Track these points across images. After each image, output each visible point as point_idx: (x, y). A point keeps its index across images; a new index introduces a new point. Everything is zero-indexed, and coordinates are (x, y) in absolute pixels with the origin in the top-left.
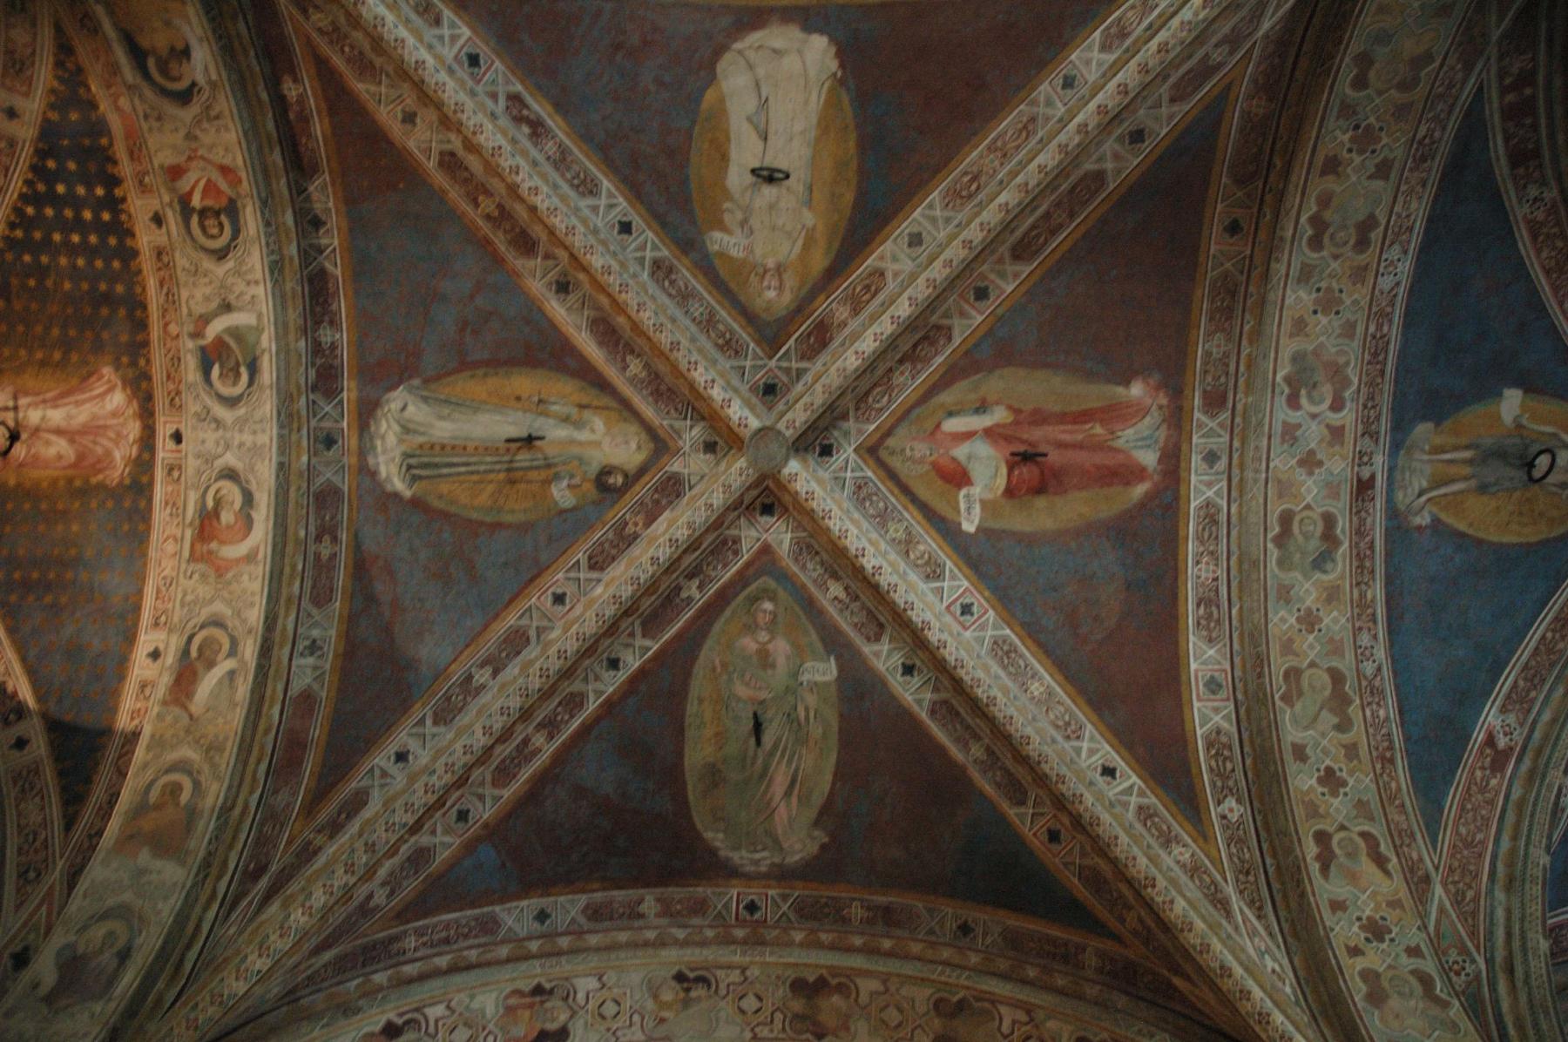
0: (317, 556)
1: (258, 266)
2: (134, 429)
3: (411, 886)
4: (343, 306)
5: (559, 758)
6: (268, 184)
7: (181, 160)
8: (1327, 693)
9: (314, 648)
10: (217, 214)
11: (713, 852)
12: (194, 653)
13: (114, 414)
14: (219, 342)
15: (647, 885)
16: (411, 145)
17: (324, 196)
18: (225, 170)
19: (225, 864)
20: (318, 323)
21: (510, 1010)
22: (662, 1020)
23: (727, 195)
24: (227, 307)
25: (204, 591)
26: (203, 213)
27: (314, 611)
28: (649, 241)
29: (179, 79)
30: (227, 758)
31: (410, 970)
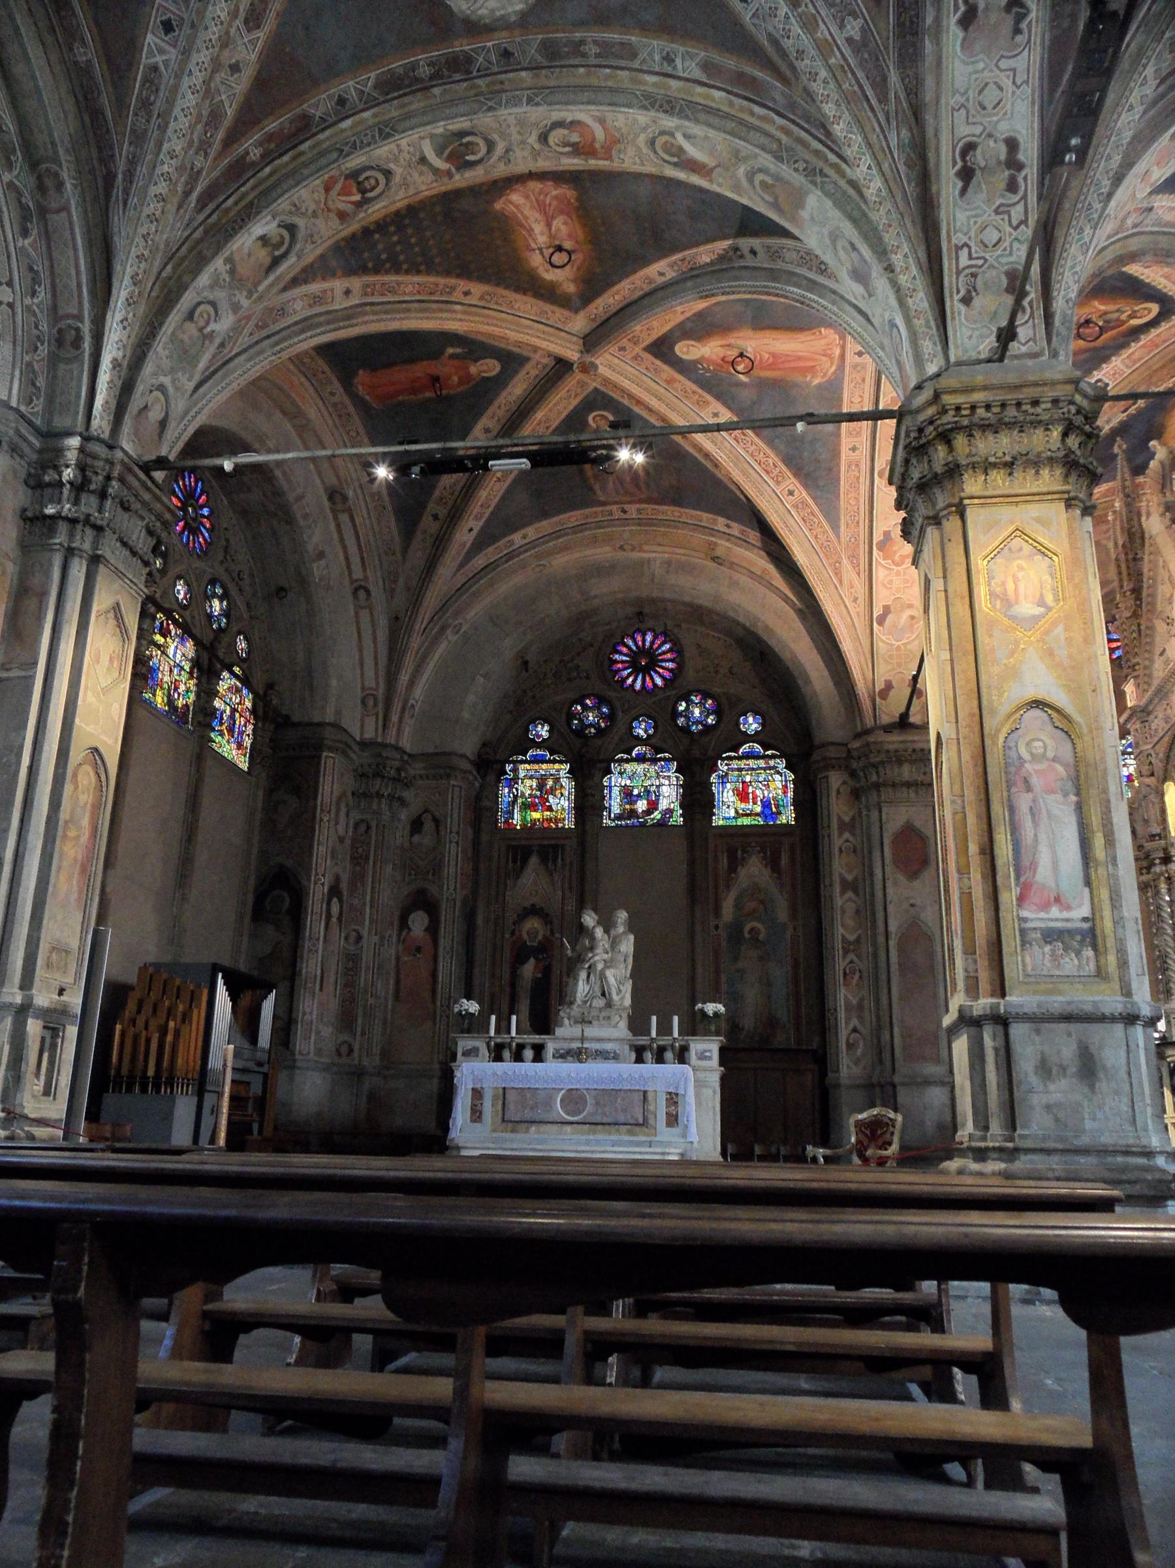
0: (597, 56)
1: (386, 148)
2: (534, 186)
4: (397, 65)
6: (328, 151)
7: (333, 215)
9: (669, 59)
10: (359, 183)
12: (675, 160)
13: (527, 197)
14: (449, 159)
16: (253, 57)
17: (319, 104)
18: (327, 190)
19: (817, 153)
20: (417, 80)
24: (423, 160)
25: (631, 151)
26: (363, 192)
27: (640, 57)
29: (282, 237)
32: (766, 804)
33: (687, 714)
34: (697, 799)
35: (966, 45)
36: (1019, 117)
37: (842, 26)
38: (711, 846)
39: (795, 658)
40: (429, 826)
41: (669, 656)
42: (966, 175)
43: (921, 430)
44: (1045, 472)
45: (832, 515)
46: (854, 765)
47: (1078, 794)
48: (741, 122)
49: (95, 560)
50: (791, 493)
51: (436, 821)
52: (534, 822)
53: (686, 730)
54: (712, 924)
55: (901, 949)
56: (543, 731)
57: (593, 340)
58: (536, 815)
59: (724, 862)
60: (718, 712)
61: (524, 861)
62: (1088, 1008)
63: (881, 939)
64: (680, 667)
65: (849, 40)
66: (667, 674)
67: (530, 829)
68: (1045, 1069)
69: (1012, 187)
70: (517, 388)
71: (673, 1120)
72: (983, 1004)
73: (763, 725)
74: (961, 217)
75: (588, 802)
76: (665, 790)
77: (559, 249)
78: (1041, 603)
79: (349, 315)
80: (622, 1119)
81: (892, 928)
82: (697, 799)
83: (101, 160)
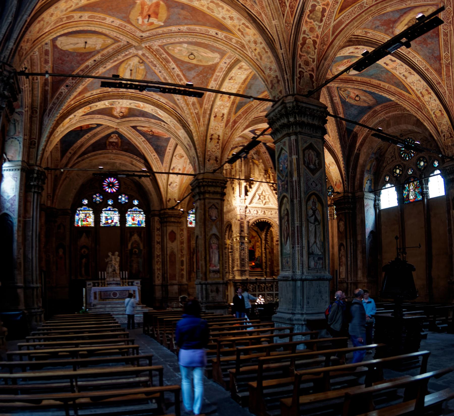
8: (215, 5)
11: (213, 64)
21: (222, 100)
30: (171, 118)
32: (139, 222)
34: (123, 220)
35: (214, 120)
39: (149, 190)
45: (162, 162)
46: (161, 216)
53: (121, 203)
55: (170, 258)
59: (129, 235)
60: (128, 199)
63: (165, 255)
82: (123, 220)
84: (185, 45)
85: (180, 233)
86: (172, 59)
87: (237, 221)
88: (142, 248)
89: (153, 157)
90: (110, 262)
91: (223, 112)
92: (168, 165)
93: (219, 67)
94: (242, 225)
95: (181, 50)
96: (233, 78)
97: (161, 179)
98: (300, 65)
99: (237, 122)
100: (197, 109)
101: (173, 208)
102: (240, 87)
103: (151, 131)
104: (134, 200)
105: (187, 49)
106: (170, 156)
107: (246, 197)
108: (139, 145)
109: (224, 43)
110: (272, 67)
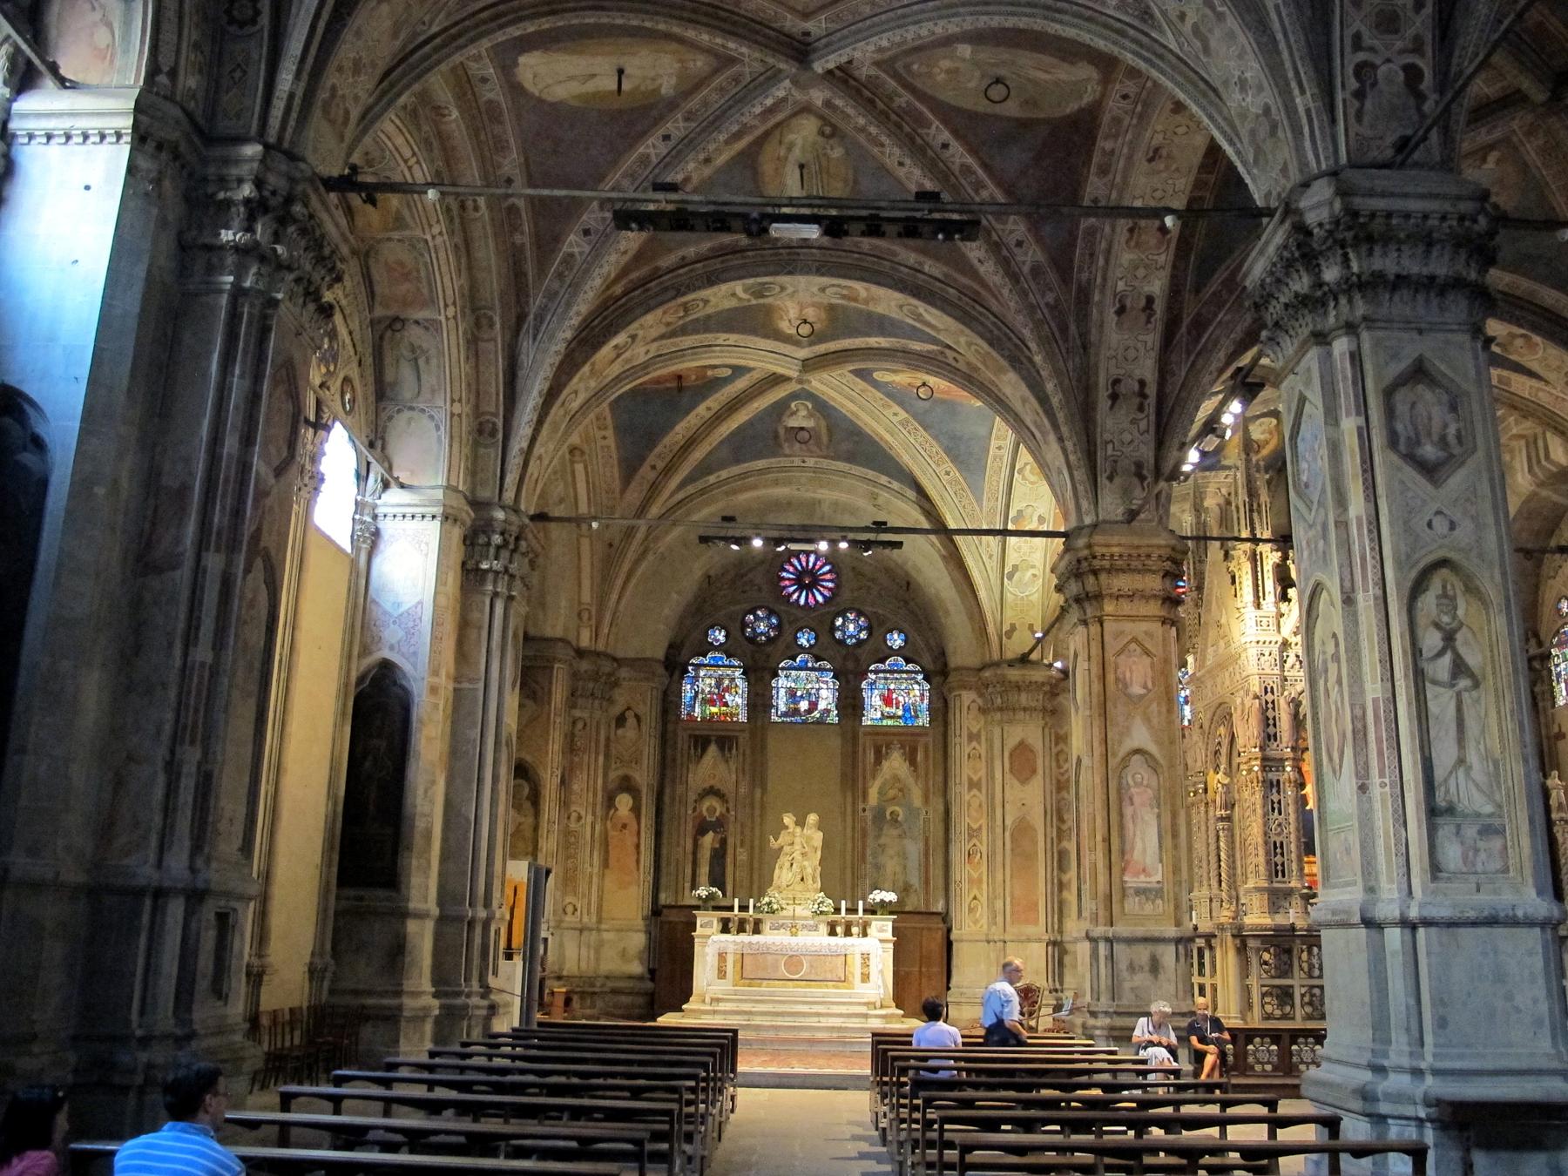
3: (1052, 277)
5: (999, 183)
6: (666, 289)
11: (1081, 110)
15: (1094, 144)
21: (1137, 245)
22: (1177, 169)
23: (637, 88)
24: (734, 295)
28: (676, 126)
30: (967, 331)
31: (1099, 280)
33: (843, 627)
34: (851, 703)
36: (1146, 369)
37: (1043, 296)
38: (861, 741)
40: (631, 721)
41: (828, 576)
42: (1114, 397)
43: (1079, 561)
44: (1152, 602)
47: (1159, 807)
48: (966, 313)
49: (510, 598)
50: (948, 473)
51: (637, 717)
52: (712, 715)
53: (842, 642)
54: (861, 806)
56: (720, 636)
57: (808, 365)
58: (714, 710)
59: (871, 756)
60: (870, 629)
61: (704, 750)
62: (1157, 934)
63: (999, 830)
64: (838, 586)
65: (1047, 304)
66: (826, 593)
67: (709, 720)
68: (1132, 968)
69: (1141, 408)
70: (741, 384)
71: (865, 978)
72: (1100, 931)
73: (906, 641)
74: (1109, 423)
75: (759, 701)
76: (824, 693)
77: (805, 322)
78: (1145, 687)
79: (645, 366)
80: (829, 977)
81: (1008, 822)
82: (851, 703)
83: (518, 302)
84: (965, 50)
85: (1054, 751)
86: (932, 110)
87: (1248, 701)
88: (917, 801)
89: (945, 478)
90: (787, 849)
91: (1147, 289)
92: (1000, 505)
93: (1106, 119)
94: (1270, 714)
95: (957, 71)
96: (1164, 152)
97: (978, 555)
98: (1357, 37)
99: (1209, 322)
100: (1051, 290)
101: (1024, 660)
102: (1198, 184)
103: (924, 384)
104: (891, 631)
105: (977, 64)
106: (1005, 472)
107: (1284, 607)
108: (888, 437)
109: (1080, 16)
110: (1248, 75)
